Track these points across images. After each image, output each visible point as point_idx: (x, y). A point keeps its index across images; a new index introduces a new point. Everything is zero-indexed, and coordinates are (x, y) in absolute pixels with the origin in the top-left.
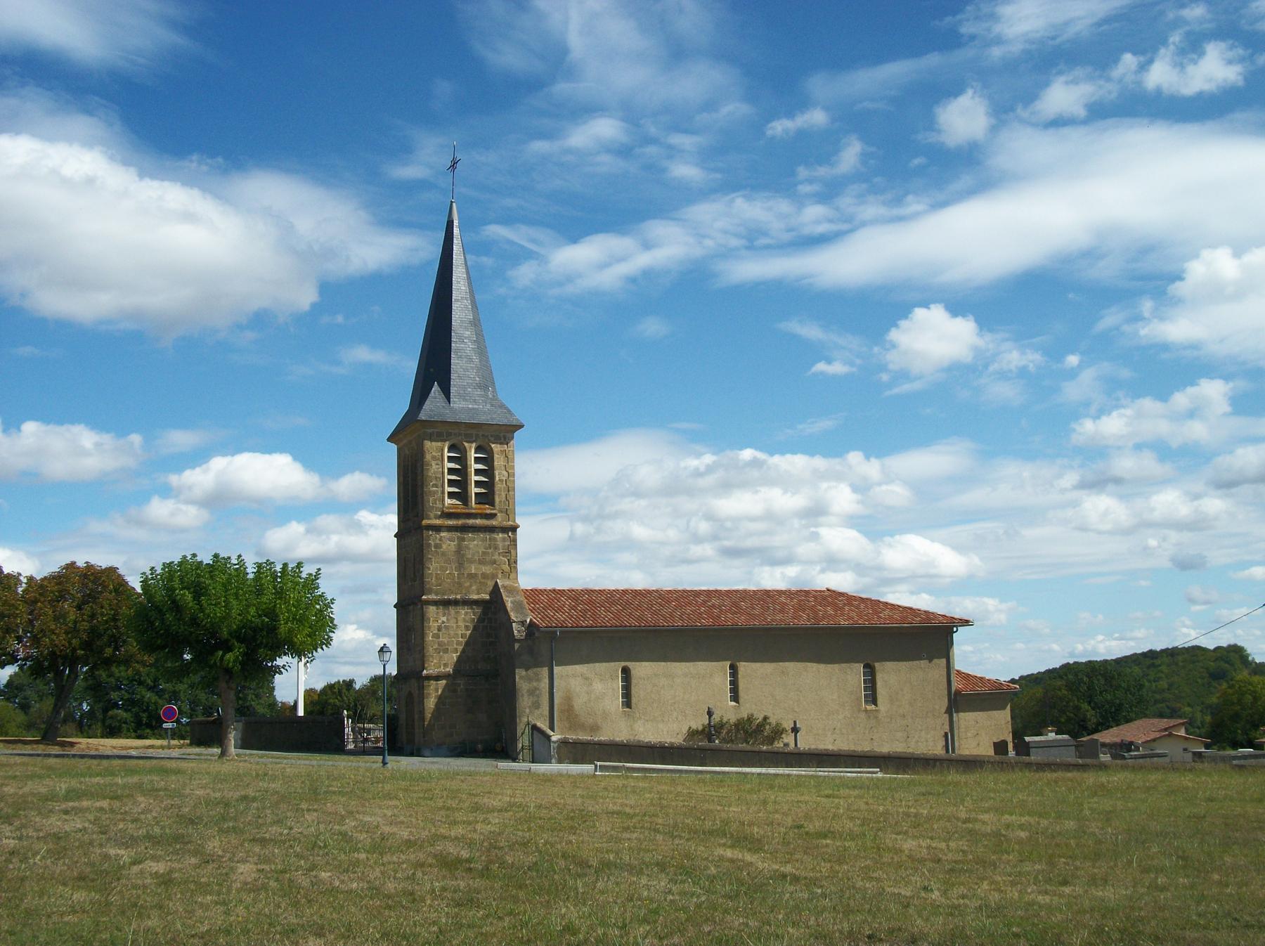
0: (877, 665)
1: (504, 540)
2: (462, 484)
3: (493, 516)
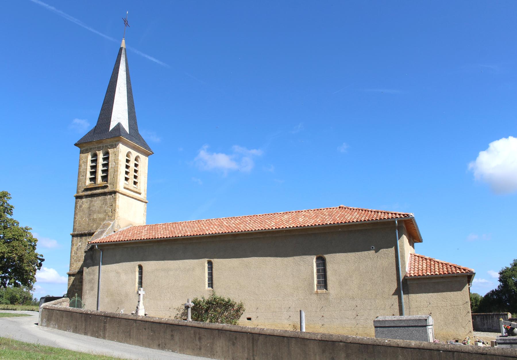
0: (326, 256)
1: (110, 198)
2: (94, 173)
3: (106, 187)
